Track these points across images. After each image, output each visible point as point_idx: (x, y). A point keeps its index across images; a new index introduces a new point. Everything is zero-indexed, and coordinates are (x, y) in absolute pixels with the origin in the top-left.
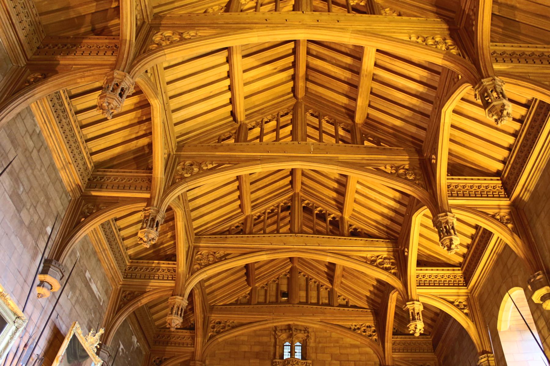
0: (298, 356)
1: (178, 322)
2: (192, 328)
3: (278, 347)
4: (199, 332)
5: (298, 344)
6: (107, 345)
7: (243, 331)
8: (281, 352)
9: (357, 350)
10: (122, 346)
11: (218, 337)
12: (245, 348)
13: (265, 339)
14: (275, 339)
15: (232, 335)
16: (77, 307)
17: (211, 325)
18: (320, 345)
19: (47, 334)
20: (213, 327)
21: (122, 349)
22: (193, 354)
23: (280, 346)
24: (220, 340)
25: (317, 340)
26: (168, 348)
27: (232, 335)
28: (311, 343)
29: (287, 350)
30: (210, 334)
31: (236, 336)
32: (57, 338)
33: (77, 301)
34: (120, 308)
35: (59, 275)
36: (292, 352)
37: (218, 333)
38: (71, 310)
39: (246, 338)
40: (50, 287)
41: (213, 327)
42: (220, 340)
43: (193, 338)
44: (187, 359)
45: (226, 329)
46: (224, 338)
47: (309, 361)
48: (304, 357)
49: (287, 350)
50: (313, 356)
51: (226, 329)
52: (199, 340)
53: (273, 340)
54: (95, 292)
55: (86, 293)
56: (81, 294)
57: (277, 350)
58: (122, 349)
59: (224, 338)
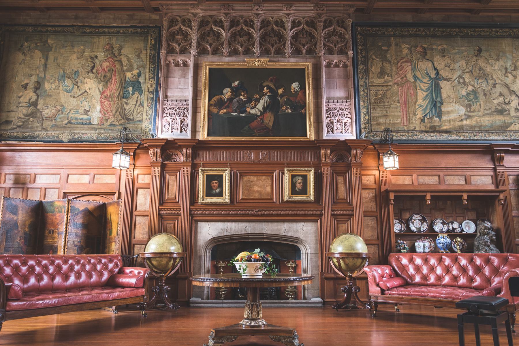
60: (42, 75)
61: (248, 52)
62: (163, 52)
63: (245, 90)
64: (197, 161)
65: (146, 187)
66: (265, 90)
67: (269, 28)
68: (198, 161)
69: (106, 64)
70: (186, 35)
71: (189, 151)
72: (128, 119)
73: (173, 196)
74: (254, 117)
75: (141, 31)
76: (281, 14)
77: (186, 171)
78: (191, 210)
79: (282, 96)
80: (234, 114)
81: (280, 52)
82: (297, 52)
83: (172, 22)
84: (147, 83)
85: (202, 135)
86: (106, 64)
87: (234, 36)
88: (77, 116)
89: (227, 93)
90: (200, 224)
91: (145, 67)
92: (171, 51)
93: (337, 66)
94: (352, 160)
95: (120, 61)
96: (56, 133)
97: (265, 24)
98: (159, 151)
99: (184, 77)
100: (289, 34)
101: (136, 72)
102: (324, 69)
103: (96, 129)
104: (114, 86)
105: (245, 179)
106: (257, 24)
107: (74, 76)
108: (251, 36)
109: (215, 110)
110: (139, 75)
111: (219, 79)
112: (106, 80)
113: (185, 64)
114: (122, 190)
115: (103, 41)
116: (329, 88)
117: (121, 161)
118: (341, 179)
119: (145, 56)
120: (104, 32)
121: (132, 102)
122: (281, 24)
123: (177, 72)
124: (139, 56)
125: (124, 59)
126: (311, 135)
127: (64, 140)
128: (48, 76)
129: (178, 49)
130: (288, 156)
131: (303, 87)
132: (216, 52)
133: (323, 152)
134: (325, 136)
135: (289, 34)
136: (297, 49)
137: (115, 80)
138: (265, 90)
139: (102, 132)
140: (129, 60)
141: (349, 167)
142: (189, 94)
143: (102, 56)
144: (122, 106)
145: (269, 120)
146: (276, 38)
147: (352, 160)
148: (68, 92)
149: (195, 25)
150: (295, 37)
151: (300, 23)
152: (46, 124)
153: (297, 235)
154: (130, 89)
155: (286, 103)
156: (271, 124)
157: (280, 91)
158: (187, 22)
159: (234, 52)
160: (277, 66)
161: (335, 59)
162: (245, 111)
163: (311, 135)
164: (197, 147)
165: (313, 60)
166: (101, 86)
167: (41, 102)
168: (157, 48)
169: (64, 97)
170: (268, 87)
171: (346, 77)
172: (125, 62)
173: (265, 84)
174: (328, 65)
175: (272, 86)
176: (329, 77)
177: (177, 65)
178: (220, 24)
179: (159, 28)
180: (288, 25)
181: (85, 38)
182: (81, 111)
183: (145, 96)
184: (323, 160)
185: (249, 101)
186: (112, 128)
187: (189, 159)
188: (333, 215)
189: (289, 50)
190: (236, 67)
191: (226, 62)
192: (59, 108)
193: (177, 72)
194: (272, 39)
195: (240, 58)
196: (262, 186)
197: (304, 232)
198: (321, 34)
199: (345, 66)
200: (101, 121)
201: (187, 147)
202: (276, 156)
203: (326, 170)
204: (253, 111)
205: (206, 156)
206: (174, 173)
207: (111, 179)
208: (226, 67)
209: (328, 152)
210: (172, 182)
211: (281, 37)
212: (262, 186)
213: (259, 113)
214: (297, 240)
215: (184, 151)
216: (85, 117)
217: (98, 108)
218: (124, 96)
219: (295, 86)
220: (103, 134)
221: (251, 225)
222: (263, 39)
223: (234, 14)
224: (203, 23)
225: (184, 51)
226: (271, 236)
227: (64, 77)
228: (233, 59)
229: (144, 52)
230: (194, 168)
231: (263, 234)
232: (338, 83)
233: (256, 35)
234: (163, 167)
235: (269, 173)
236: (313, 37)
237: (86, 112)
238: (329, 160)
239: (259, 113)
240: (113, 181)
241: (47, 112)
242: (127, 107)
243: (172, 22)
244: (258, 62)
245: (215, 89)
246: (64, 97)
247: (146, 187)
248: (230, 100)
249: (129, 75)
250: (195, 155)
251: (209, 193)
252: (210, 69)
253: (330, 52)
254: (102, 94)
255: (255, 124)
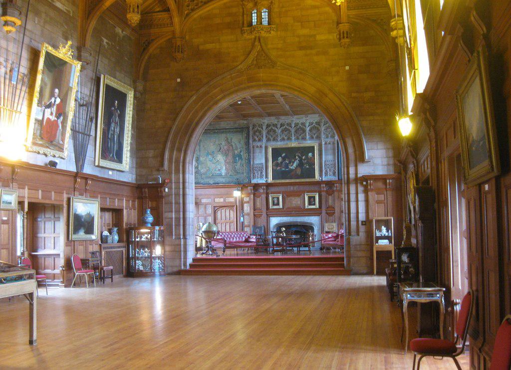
0: (265, 22)
1: (136, 18)
2: (168, 10)
3: (245, 16)
4: (175, 13)
5: (265, 10)
6: (86, 46)
7: (215, 5)
8: (249, 19)
9: (317, 11)
10: (105, 40)
11: (192, 14)
12: (218, 21)
13: (234, 10)
14: (243, 9)
15: (205, 10)
16: (48, 27)
17: (186, 4)
18: (284, 10)
19: (25, 55)
20: (188, 6)
21: (107, 43)
22: (173, 32)
23: (247, 15)
24: (196, 16)
25: (281, 5)
26: (152, 31)
27: (205, 10)
28: (276, 9)
29: (254, 16)
30: (186, 12)
31: (209, 11)
32: (35, 55)
33: (45, 22)
34: (90, 13)
35: (17, 13)
36: (260, 18)
37: (193, 10)
38: (42, 31)
39: (217, 11)
40: (13, 24)
41: (188, 6)
42: (196, 16)
43: (171, 18)
44: (169, 37)
45: (200, 5)
46: (199, 14)
47: (273, 26)
48: (269, 23)
49: (254, 16)
50: (277, 20)
51: (200, 5)
52: (176, 20)
53: (241, 10)
54: (62, 8)
55: (52, 13)
56: (47, 15)
57: (245, 18)
58: (107, 43)
59: (199, 14)
60: (198, 154)
61: (289, 139)
62: (251, 141)
63: (289, 158)
64: (268, 191)
65: (248, 202)
66: (297, 157)
67: (298, 127)
68: (268, 191)
69: (226, 147)
70: (260, 132)
71: (265, 187)
72: (237, 173)
73: (259, 207)
74: (292, 170)
75: (240, 130)
76: (303, 120)
77: (264, 196)
78: (267, 213)
79: (304, 160)
80: (283, 169)
81: (304, 139)
82: (312, 138)
83: (254, 126)
84: (244, 155)
85: (270, 180)
86: (226, 147)
87: (282, 131)
88: (216, 172)
89: (280, 159)
90: (271, 218)
91: (243, 148)
92: (254, 140)
93: (330, 144)
94: (335, 189)
95: (232, 146)
96: (208, 180)
97: (296, 125)
98: (252, 188)
99: (261, 152)
100: (308, 129)
101: (239, 150)
102: (323, 146)
103: (224, 178)
104: (230, 158)
105: (289, 198)
106: (293, 125)
107: (212, 154)
108: (291, 131)
109: (275, 168)
110: (241, 152)
111: (276, 152)
112: (226, 154)
113: (261, 147)
114: (238, 204)
115: (223, 136)
116: (326, 155)
117: (237, 194)
118: (330, 197)
119: (243, 142)
120: (223, 132)
121: (239, 164)
122: (303, 124)
123: (257, 150)
124: (240, 142)
125: (233, 144)
126: (317, 177)
127: (211, 183)
128: (201, 154)
129: (257, 139)
130: (307, 188)
131: (314, 155)
132: (274, 140)
133: (322, 185)
134: (324, 179)
135: (308, 129)
136: (311, 136)
137: (231, 154)
138: (297, 157)
139: (227, 179)
140: (235, 144)
141: (333, 191)
142: (263, 161)
143: (223, 143)
144: (234, 166)
145: (299, 171)
146: (301, 131)
147: (335, 189)
148: (211, 161)
149: (264, 127)
150: (310, 130)
151: (312, 123)
152: (203, 176)
153: (312, 222)
154: (237, 158)
155: (306, 163)
156: (300, 173)
157: (304, 158)
158: (261, 126)
159: (283, 139)
160: (302, 145)
161: (329, 140)
162: (288, 168)
163: (317, 177)
164: (268, 185)
165: (318, 141)
166: (224, 158)
167: (199, 166)
168: (248, 137)
169: (209, 163)
170: (298, 156)
171: (334, 149)
172: (234, 146)
173: (297, 154)
174: (326, 144)
175: (300, 155)
176: (326, 150)
177: (257, 147)
178: (275, 126)
179: (248, 128)
180: (307, 125)
181: (216, 135)
182: (217, 170)
183: (243, 162)
184: (322, 189)
185: (290, 163)
186: (231, 177)
187: (265, 191)
188: (326, 213)
189: (308, 137)
190: (284, 147)
191: (280, 144)
192: (207, 169)
193: (257, 150)
194: (300, 131)
195: (286, 142)
196: (295, 202)
197: (314, 220)
198: (323, 128)
199: (334, 143)
200: (226, 174)
201: (264, 186)
202: (302, 188)
203: (323, 194)
204: (292, 168)
205: (272, 189)
206: (259, 197)
207: (232, 200)
208: (279, 147)
209: (324, 185)
210: (258, 200)
211: (304, 131)
212: (295, 202)
213: (294, 168)
214: (311, 224)
215: (263, 187)
216: (219, 172)
217: (224, 168)
218: (235, 162)
219: (310, 155)
220: (228, 180)
221: (292, 218)
222: (296, 131)
223: (281, 121)
224: (268, 126)
225: (260, 140)
226: (300, 222)
227: (208, 154)
228: (282, 143)
229: (242, 141)
230: (267, 194)
231: (297, 222)
232: (330, 152)
233: (293, 131)
234: (254, 195)
235: (299, 196)
236: (318, 130)
237: (219, 170)
238: (325, 189)
239: (294, 168)
240: (233, 201)
241: (202, 171)
242: (237, 167)
243: (254, 126)
244: (294, 144)
245: (275, 158)
246: (209, 163)
247: (248, 202)
248: (282, 162)
249: (236, 152)
250: (267, 189)
251: (274, 205)
252: (273, 149)
253: (327, 137)
254: (225, 161)
255: (293, 173)
